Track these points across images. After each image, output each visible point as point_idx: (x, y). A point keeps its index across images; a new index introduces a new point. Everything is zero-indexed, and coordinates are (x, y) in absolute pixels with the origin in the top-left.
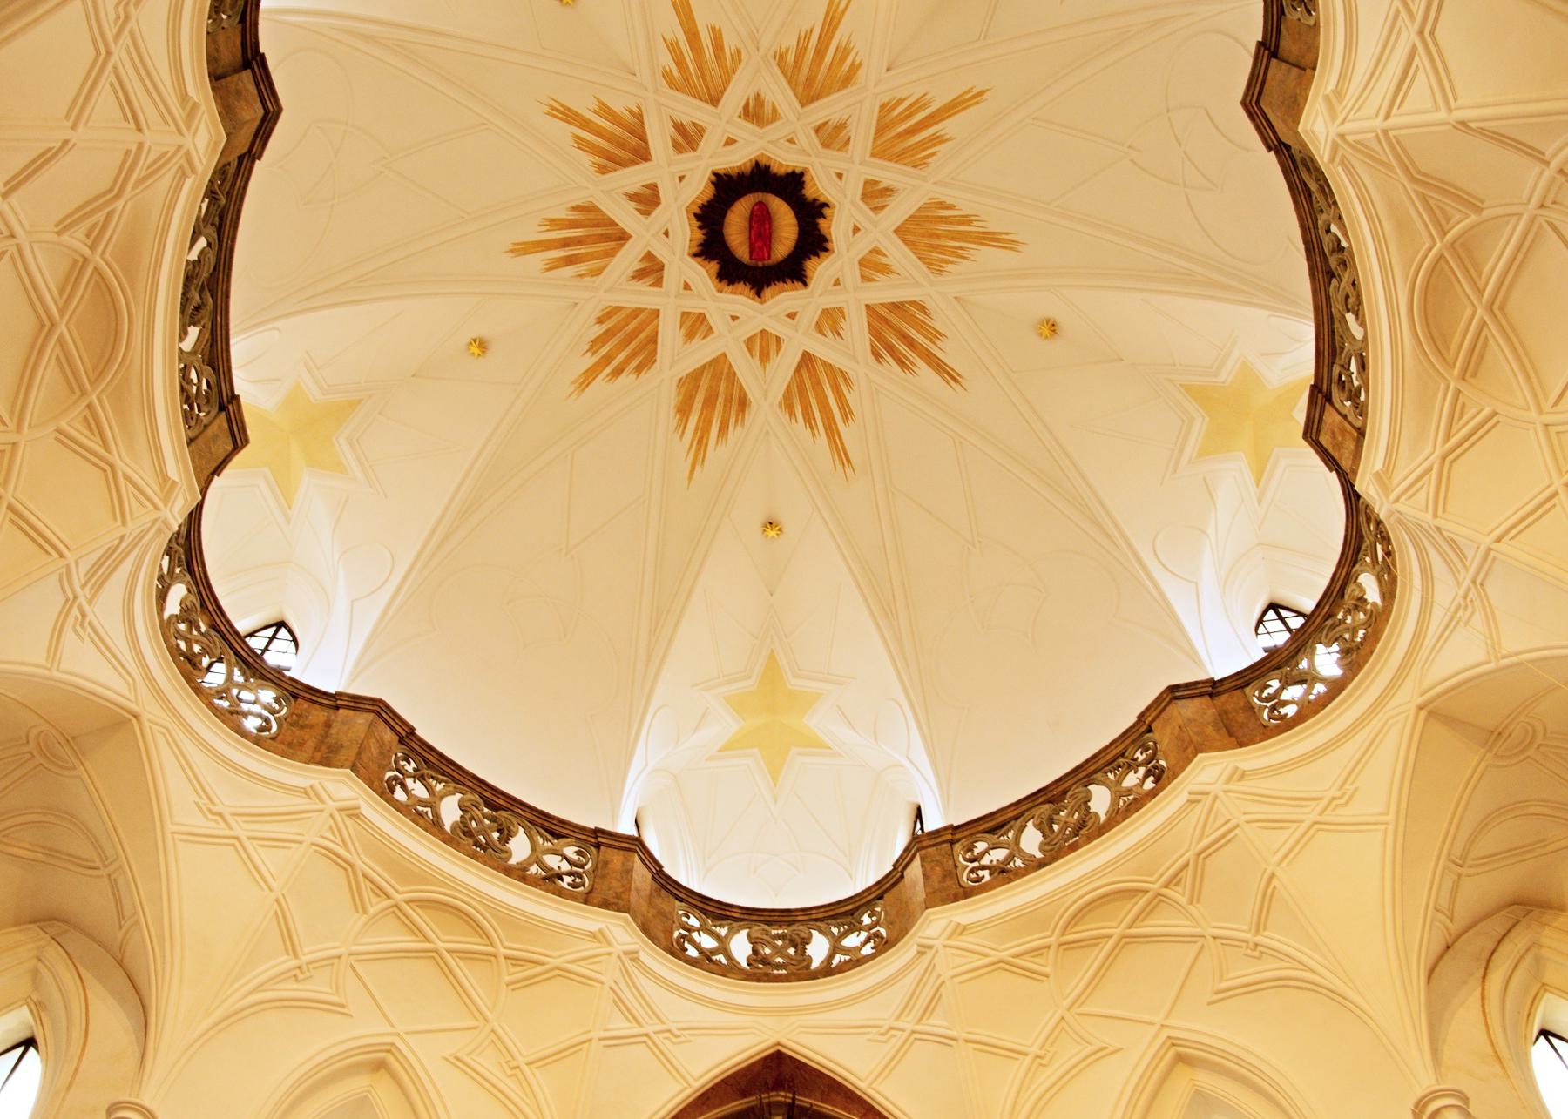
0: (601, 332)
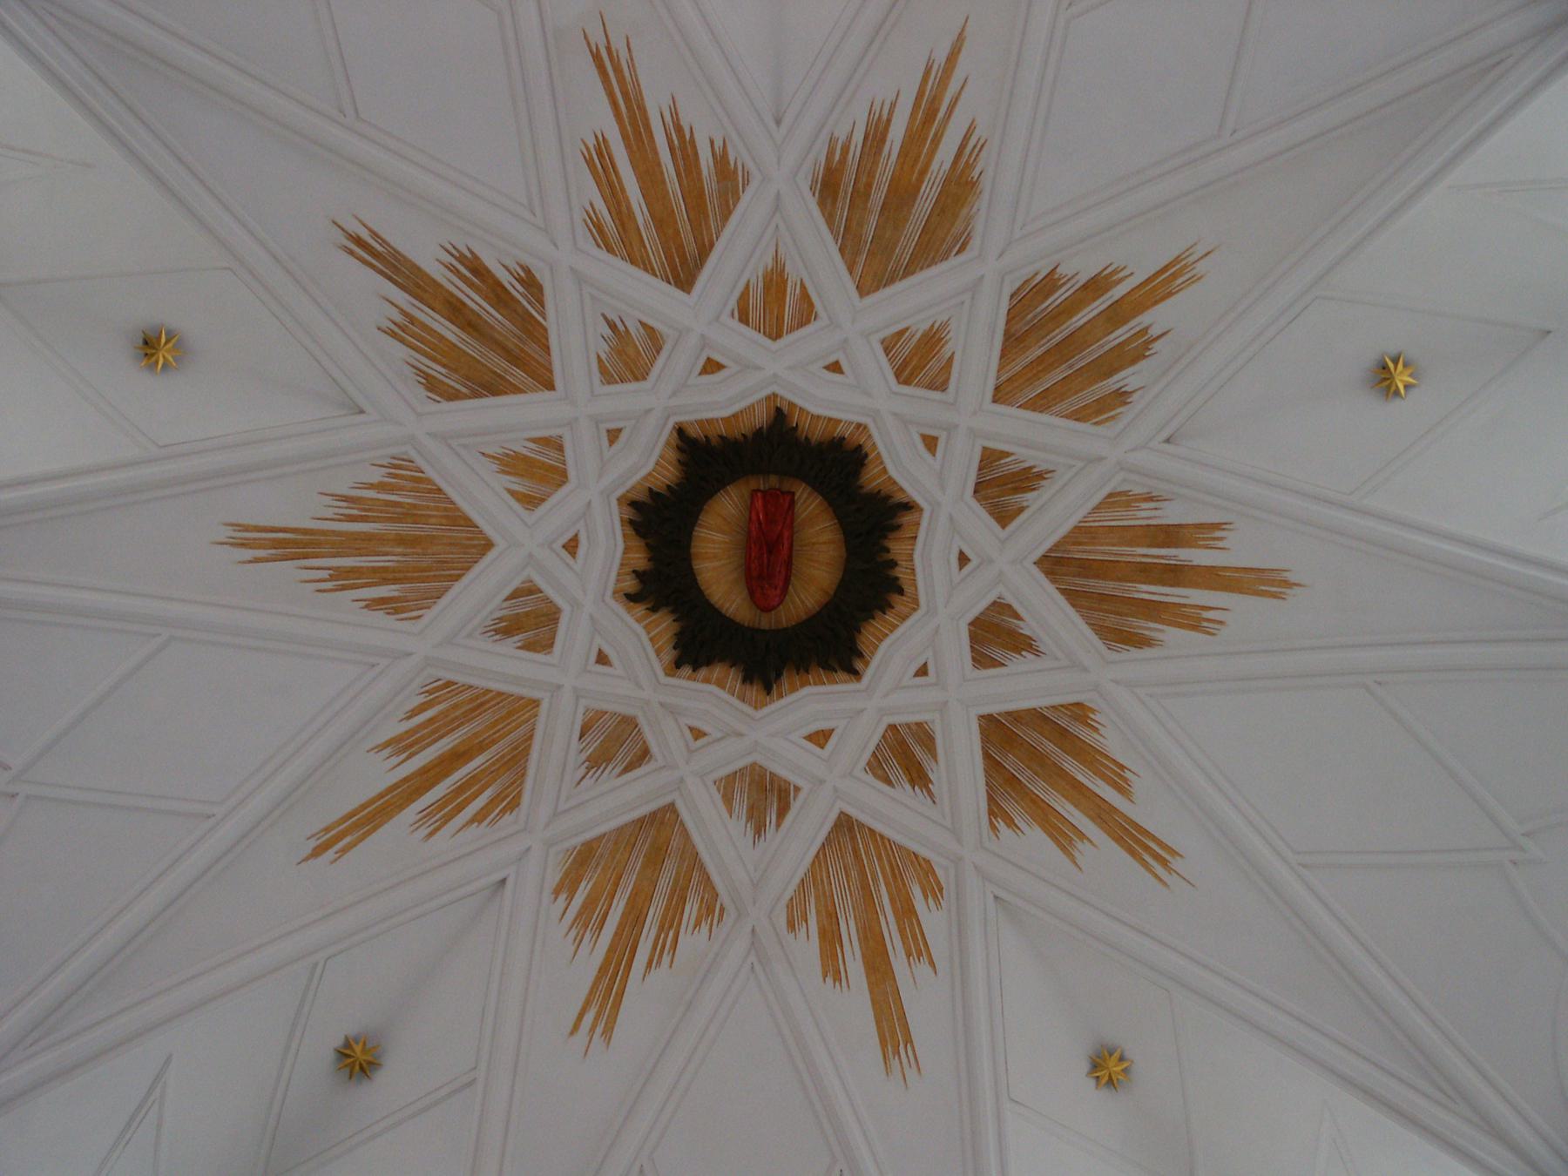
0: (1123, 374)
